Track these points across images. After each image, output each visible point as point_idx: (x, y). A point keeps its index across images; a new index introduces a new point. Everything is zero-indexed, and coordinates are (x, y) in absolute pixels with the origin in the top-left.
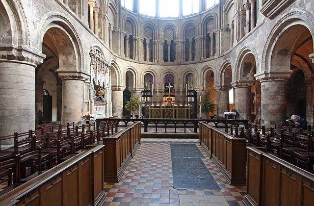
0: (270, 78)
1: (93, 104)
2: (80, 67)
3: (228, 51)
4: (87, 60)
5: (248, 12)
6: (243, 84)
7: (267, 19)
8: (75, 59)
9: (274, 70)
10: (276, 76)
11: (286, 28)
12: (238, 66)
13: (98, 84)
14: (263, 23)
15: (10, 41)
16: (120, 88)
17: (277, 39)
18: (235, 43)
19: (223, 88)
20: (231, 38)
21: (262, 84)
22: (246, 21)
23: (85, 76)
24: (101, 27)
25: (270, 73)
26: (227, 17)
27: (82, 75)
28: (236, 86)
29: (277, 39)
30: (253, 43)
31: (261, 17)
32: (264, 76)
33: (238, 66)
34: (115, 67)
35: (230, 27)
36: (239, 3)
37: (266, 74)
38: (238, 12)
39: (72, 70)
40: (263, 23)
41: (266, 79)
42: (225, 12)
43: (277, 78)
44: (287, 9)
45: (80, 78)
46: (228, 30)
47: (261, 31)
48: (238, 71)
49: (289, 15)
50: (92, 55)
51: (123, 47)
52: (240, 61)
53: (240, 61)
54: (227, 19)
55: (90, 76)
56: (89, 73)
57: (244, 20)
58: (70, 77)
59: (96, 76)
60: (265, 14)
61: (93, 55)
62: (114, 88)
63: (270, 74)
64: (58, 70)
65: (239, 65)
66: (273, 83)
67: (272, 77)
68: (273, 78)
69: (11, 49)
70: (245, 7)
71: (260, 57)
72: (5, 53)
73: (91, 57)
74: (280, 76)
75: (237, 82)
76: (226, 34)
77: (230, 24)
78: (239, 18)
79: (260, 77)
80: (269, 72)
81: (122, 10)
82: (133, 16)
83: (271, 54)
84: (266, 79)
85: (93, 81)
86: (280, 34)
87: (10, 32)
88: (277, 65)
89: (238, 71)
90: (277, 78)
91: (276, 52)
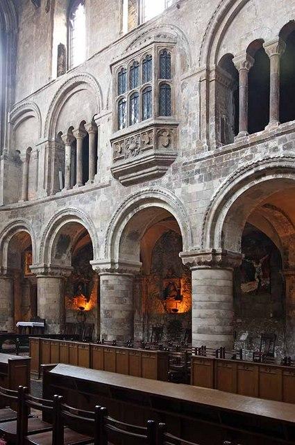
0: (118, 271)
3: (22, 203)
5: (68, 149)
6: (56, 271)
7: (115, 182)
9: (123, 260)
10: (124, 268)
11: (145, 206)
12: (49, 239)
14: (109, 185)
17: (130, 216)
18: (38, 193)
19: (5, 272)
20: (24, 178)
21: (102, 278)
22: (62, 161)
25: (119, 263)
26: (15, 134)
28: (41, 273)
29: (130, 216)
30: (88, 208)
31: (104, 174)
32: (109, 266)
33: (49, 239)
35: (23, 156)
36: (51, 126)
37: (113, 263)
38: (50, 141)
40: (107, 186)
41: (111, 271)
42: (12, 123)
43: (125, 271)
44: (150, 183)
46: (17, 161)
47: (102, 196)
48: (47, 247)
49: (151, 191)
52: (53, 229)
53: (53, 229)
54: (15, 137)
57: (60, 160)
60: (116, 175)
63: (117, 265)
65: (50, 235)
66: (120, 278)
67: (118, 270)
68: (120, 271)
70: (64, 137)
71: (102, 235)
74: (129, 268)
75: (46, 267)
76: (12, 167)
77: (24, 152)
78: (50, 152)
79: (101, 267)
80: (116, 260)
83: (119, 234)
84: (111, 271)
86: (135, 211)
88: (126, 252)
89: (47, 247)
90: (125, 271)
91: (126, 234)
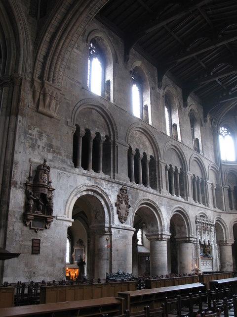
1: (200, 260)
2: (189, 234)
4: (193, 226)
8: (186, 228)
13: (203, 243)
15: (158, 231)
16: (227, 242)
23: (193, 239)
24: (204, 193)
27: (191, 239)
34: (221, 222)
39: (184, 236)
45: (189, 241)
50: (196, 222)
51: (227, 201)
55: (197, 238)
56: (196, 237)
58: (183, 241)
59: (201, 237)
61: (198, 222)
62: (221, 243)
64: (175, 237)
69: (159, 235)
72: (156, 237)
73: (196, 223)
81: (222, 166)
82: (234, 167)
85: (200, 241)
87: (158, 228)
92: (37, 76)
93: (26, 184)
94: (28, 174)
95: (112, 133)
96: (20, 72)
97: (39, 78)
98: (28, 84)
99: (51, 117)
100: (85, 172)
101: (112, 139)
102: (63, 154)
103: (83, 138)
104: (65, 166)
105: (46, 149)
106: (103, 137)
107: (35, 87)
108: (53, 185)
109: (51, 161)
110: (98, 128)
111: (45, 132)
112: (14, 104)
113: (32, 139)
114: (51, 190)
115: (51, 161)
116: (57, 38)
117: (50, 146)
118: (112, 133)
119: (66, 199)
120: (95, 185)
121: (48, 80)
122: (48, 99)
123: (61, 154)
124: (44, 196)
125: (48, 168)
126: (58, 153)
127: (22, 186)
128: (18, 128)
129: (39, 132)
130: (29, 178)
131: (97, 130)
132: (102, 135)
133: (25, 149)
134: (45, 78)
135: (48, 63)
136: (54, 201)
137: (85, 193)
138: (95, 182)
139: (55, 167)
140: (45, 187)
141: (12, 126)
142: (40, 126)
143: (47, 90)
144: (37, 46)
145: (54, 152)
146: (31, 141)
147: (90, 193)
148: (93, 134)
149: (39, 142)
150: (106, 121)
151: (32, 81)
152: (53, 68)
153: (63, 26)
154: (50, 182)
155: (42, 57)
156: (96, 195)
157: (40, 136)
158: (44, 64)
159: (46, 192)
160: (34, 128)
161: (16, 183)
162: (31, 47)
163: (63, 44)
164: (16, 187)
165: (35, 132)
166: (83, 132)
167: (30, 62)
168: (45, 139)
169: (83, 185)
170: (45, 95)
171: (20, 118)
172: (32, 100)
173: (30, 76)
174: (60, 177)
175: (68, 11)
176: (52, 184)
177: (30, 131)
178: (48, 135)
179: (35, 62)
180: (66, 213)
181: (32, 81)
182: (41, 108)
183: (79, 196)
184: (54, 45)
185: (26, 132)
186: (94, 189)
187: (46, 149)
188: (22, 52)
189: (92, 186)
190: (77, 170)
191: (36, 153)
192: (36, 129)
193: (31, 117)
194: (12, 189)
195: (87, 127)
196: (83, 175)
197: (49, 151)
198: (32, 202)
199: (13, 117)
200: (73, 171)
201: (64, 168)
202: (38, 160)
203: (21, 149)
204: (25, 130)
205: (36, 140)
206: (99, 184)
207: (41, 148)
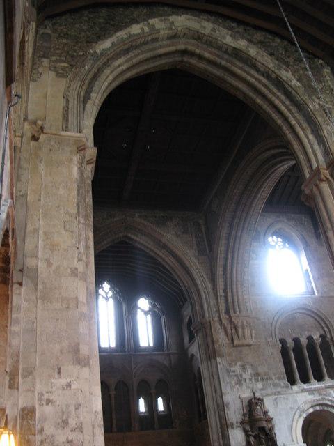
92: (223, 311)
93: (242, 423)
94: (242, 411)
95: (326, 329)
96: (207, 315)
97: (225, 313)
98: (218, 325)
99: (249, 346)
100: (305, 386)
101: (329, 336)
102: (274, 378)
103: (294, 350)
104: (279, 389)
105: (253, 380)
106: (317, 339)
107: (224, 325)
108: (271, 414)
109: (262, 389)
110: (308, 331)
111: (248, 363)
112: (211, 347)
113: (236, 376)
114: (269, 420)
115: (262, 389)
116: (229, 268)
117: (257, 374)
118: (326, 329)
119: (289, 424)
120: (320, 397)
121: (235, 312)
122: (240, 331)
123: (270, 379)
124: (262, 429)
125: (258, 399)
126: (267, 379)
127: (239, 424)
128: (219, 371)
129: (242, 366)
130: (244, 415)
131: (307, 334)
132: (315, 337)
133: (232, 388)
134: (231, 311)
135: (229, 294)
136: (277, 431)
137: (311, 410)
138: (320, 394)
139: (267, 395)
140: (261, 420)
141: (214, 370)
142: (241, 359)
143: (236, 322)
144: (213, 281)
145: (262, 380)
146: (235, 378)
147: (318, 408)
148: (304, 341)
149: (245, 376)
150: (316, 319)
151: (220, 320)
152: (235, 298)
153: (229, 255)
154: (265, 413)
155: (222, 291)
156: (325, 408)
157: (244, 368)
158: (226, 297)
159: (264, 424)
160: (236, 364)
161: (232, 424)
162: (209, 286)
163: (237, 271)
164: (233, 428)
165: (237, 368)
166: (290, 343)
167: (213, 301)
168: (249, 371)
169: (306, 403)
170: (236, 328)
171: (219, 360)
172: (225, 337)
173: (217, 315)
174: (277, 403)
175: (228, 240)
176: (269, 414)
177: (232, 369)
178: (252, 365)
179: (217, 299)
180: (294, 439)
181: (220, 320)
182: (236, 342)
183: (305, 415)
184: (229, 275)
185: (228, 371)
186: (320, 402)
187: (253, 380)
188: (203, 297)
189: (317, 400)
190: (295, 388)
191: (244, 387)
192: (238, 364)
193: (230, 355)
194: (230, 432)
195: (295, 336)
196: (303, 391)
197: (257, 380)
198: (252, 439)
199: (213, 360)
200: (290, 391)
201: (278, 392)
202: (247, 394)
203: (229, 390)
204: (227, 370)
205: (241, 375)
206: (324, 395)
207: (247, 381)
